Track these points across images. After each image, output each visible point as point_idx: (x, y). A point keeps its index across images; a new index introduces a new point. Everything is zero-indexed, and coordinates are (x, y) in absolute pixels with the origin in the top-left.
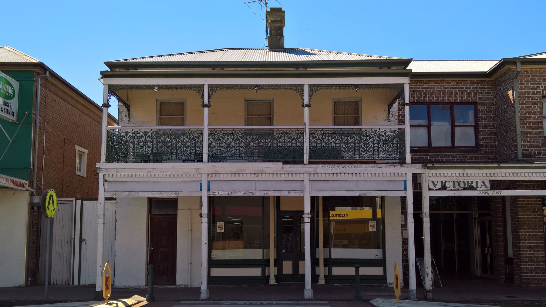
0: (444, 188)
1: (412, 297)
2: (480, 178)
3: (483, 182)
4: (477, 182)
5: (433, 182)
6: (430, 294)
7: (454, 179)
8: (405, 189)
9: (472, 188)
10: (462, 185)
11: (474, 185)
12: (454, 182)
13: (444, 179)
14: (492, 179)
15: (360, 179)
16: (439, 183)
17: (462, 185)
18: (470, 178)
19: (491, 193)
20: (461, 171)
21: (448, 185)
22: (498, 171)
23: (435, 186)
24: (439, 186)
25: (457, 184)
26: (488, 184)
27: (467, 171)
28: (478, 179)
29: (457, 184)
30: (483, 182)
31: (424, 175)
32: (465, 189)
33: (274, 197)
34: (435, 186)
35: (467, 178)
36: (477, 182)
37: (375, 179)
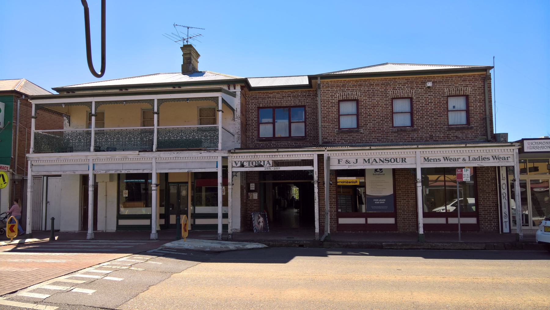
0: (242, 166)
1: (219, 238)
2: (266, 159)
3: (268, 161)
4: (264, 161)
5: (235, 162)
6: (231, 236)
7: (249, 160)
8: (217, 167)
9: (261, 166)
10: (254, 164)
11: (262, 164)
12: (249, 162)
13: (242, 160)
14: (274, 159)
15: (188, 161)
16: (239, 163)
17: (254, 164)
18: (259, 159)
19: (273, 169)
20: (253, 154)
21: (245, 164)
22: (277, 154)
23: (236, 164)
24: (239, 165)
25: (251, 163)
26: (271, 163)
27: (257, 154)
28: (264, 159)
29: (251, 163)
30: (268, 161)
31: (229, 158)
32: (256, 166)
33: (192, 173)
34: (236, 164)
35: (257, 159)
36: (264, 161)
37: (197, 160)
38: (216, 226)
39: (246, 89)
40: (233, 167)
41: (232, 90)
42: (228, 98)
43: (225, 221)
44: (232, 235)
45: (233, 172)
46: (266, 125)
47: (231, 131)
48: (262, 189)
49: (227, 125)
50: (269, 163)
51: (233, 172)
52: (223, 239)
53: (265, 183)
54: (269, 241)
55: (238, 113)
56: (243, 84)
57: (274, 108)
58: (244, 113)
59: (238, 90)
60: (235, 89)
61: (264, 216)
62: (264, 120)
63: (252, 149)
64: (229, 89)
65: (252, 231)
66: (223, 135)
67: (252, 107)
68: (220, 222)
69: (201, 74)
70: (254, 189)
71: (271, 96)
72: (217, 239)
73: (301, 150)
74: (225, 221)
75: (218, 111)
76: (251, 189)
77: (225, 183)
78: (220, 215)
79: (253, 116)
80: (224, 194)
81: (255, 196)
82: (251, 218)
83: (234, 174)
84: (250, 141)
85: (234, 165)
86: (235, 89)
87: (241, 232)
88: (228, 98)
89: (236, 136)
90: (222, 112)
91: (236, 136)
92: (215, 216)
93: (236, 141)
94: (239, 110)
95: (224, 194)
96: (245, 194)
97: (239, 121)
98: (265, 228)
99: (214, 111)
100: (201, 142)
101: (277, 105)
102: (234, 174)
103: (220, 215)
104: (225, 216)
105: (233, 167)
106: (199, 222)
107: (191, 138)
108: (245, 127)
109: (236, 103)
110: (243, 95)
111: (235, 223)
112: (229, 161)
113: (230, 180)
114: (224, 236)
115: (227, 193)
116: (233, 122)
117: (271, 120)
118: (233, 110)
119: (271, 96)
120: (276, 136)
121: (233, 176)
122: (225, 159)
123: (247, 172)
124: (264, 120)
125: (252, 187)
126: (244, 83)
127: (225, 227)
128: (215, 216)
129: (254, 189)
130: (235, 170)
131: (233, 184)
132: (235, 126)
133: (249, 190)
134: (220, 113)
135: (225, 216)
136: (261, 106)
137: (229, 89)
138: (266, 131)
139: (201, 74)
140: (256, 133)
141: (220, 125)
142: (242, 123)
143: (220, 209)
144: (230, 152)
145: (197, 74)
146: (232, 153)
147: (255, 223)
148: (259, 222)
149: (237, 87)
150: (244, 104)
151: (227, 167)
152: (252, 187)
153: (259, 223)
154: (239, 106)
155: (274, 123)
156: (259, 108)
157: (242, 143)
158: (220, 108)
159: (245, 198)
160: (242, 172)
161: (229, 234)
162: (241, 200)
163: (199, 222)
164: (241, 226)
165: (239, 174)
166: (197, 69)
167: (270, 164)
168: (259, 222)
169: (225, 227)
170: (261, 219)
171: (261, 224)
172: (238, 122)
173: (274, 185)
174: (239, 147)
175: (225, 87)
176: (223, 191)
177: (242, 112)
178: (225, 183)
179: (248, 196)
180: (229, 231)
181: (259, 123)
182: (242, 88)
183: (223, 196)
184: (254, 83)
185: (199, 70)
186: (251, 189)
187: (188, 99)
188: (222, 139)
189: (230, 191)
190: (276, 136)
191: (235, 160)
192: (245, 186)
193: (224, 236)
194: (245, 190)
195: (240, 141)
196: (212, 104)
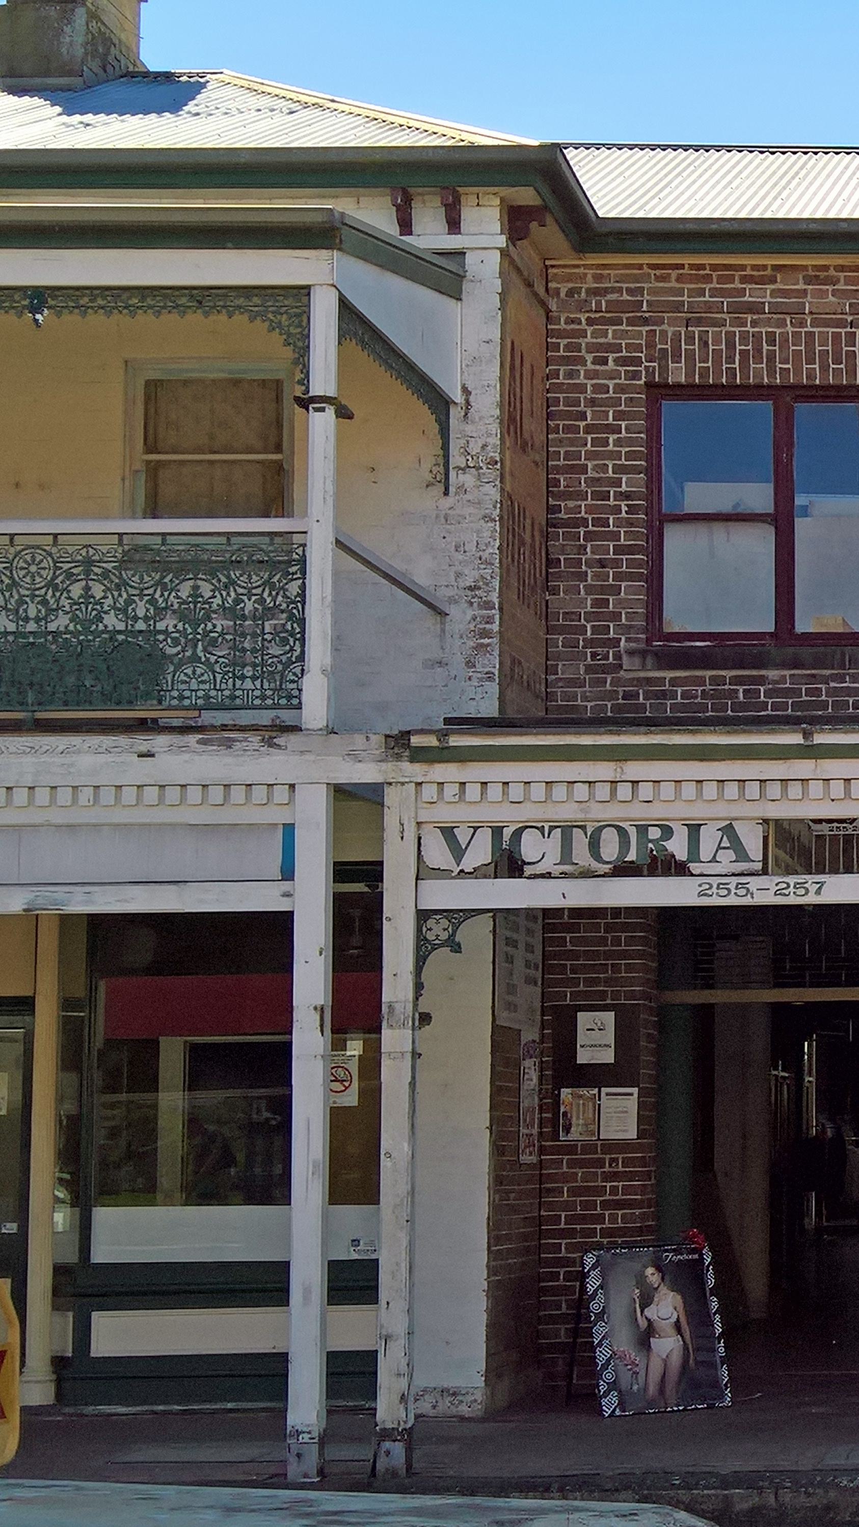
0: (510, 864)
1: (294, 1471)
2: (712, 809)
3: (728, 830)
4: (694, 830)
5: (448, 833)
6: (398, 1449)
7: (568, 813)
8: (288, 874)
9: (664, 865)
10: (610, 849)
11: (678, 847)
12: (567, 830)
13: (509, 816)
14: (776, 811)
15: (37, 817)
16: (485, 838)
17: (610, 849)
18: (657, 811)
19: (765, 892)
20: (604, 770)
21: (531, 848)
22: (803, 768)
23: (458, 852)
24: (480, 853)
25: (580, 842)
26: (753, 844)
27: (635, 769)
28: (696, 812)
29: (580, 842)
30: (728, 830)
31: (391, 796)
32: (623, 870)
34: (458, 852)
35: (639, 812)
36: (694, 830)
37: (120, 816)
38: (268, 1373)
39: (550, 234)
40: (423, 872)
41: (430, 234)
42: (391, 302)
43: (353, 1328)
44: (408, 1436)
45: (423, 916)
46: (719, 529)
47: (421, 575)
48: (683, 1062)
49: (388, 531)
50: (736, 845)
51: (423, 916)
52: (327, 1479)
53: (706, 1012)
54: (725, 1482)
55: (481, 427)
56: (526, 196)
57: (786, 397)
58: (533, 427)
59: (483, 231)
60: (454, 225)
61: (687, 1279)
62: (699, 496)
63: (598, 723)
64: (406, 226)
65: (589, 1401)
66: (342, 610)
67: (605, 380)
68: (304, 1331)
69: (170, 91)
70: (608, 1057)
71: (766, 296)
72: (277, 1480)
73: (586, 740)
74: (353, 1328)
75: (305, 402)
76: (583, 1057)
77: (356, 1009)
78: (307, 1278)
79: (610, 459)
80: (351, 1099)
81: (619, 1115)
82: (582, 1302)
83: (437, 930)
84: (583, 651)
85: (437, 854)
86: (454, 225)
87: (491, 1415)
88: (391, 302)
89: (461, 616)
90: (344, 413)
91: (461, 616)
92: (265, 1284)
93: (458, 661)
94: (488, 404)
95: (351, 1099)
96: (529, 1100)
97: (493, 493)
98: (694, 1380)
99: (277, 403)
100: (154, 661)
101: (812, 373)
102: (438, 932)
103: (307, 1278)
104: (353, 1282)
105: (423, 872)
106: (118, 1334)
107: (61, 622)
108: (538, 546)
109: (465, 341)
110: (525, 280)
111: (439, 1343)
112: (391, 820)
113: (396, 986)
114: (335, 1452)
115: (372, 1095)
116: (431, 501)
117: (759, 496)
118: (439, 403)
119: (766, 296)
120: (802, 626)
121: (423, 950)
122: (355, 803)
123: (550, 918)
124: (699, 496)
125: (596, 1037)
126: (538, 186)
127: (351, 1374)
128: (265, 1284)
129: (608, 1057)
130: (443, 895)
131: (425, 1018)
132: (456, 537)
133: (566, 1070)
134: (322, 425)
135: (353, 1282)
136: (678, 374)
137: (406, 226)
138: (714, 580)
139: (170, 91)
140: (631, 593)
141: (317, 522)
142: (511, 515)
143: (305, 1229)
144: (399, 744)
145: (118, 91)
146: (420, 755)
147: (613, 1339)
148: (645, 1325)
149: (469, 215)
150: (534, 354)
151: (373, 872)
152: (596, 1037)
153: (645, 1337)
154: (492, 372)
155: (782, 521)
156: (659, 391)
157: (510, 676)
158: (323, 381)
159: (529, 1130)
160: (503, 918)
161: (387, 1434)
162: (498, 1150)
163: (118, 1334)
164: (493, 1373)
165: (478, 937)
166: (132, 53)
167: (742, 854)
168: (645, 1325)
169: (351, 1374)
170: (667, 1306)
171: (667, 1346)
172: (480, 496)
173: (788, 1025)
174: (489, 708)
175: (374, 213)
176: (336, 1078)
177: (511, 421)
178: (356, 1009)
179: (554, 1119)
180: (388, 1409)
181: (658, 520)
182: (517, 221)
183: (339, 1119)
184: (614, 188)
185: (153, 57)
186: (583, 1057)
187: (203, 297)
188: (338, 644)
189: (394, 1076)
190: (802, 626)
191: (446, 814)
192: (530, 1035)
193: (335, 1452)
194: (537, 1066)
195: (492, 662)
196: (253, 347)
